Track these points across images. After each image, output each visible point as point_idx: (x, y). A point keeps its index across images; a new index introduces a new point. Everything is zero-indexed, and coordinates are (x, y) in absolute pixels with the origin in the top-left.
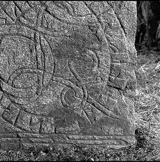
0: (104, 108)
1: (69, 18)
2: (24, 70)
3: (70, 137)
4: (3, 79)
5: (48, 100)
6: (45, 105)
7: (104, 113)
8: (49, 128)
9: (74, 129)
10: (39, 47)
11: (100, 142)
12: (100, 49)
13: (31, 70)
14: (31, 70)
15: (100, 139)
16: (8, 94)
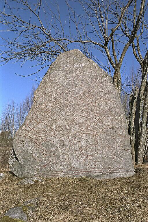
0: (121, 158)
1: (105, 127)
2: (90, 145)
3: (110, 170)
4: (83, 149)
5: (100, 156)
6: (99, 158)
7: (121, 160)
8: (101, 166)
9: (111, 167)
10: (95, 137)
11: (121, 171)
12: (117, 136)
13: (93, 145)
14: (93, 145)
15: (121, 170)
16: (85, 155)
